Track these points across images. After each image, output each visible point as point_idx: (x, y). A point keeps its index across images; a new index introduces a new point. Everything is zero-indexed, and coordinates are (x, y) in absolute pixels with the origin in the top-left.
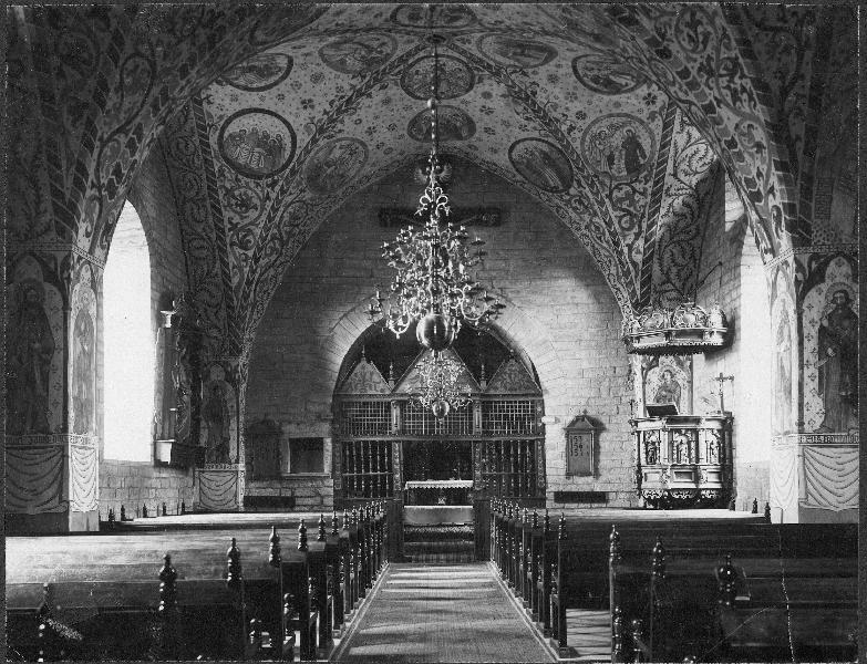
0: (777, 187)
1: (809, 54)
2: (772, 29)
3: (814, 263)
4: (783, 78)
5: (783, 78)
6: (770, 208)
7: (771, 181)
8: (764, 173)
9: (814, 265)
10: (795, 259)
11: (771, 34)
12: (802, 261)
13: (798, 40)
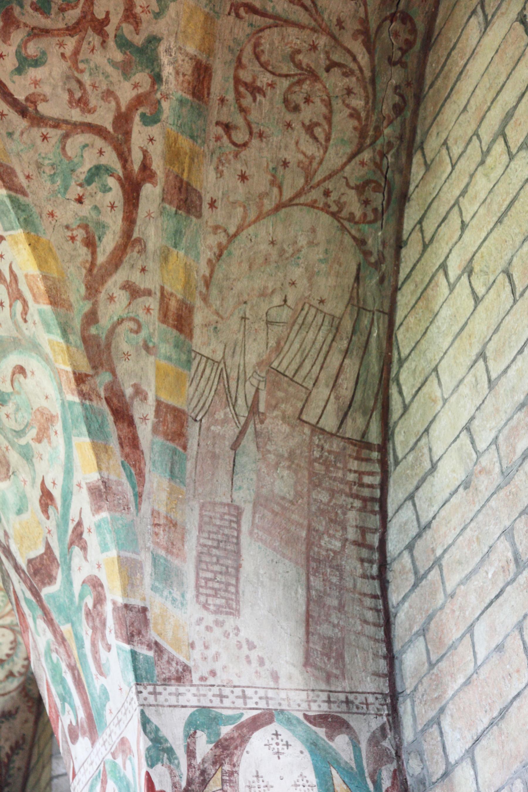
0: (90, 520)
1: (151, 193)
2: (57, 124)
3: (202, 738)
4: (91, 243)
5: (91, 243)
6: (77, 588)
7: (73, 513)
8: (57, 493)
9: (204, 747)
10: (145, 722)
11: (55, 134)
12: (165, 732)
13: (124, 158)
